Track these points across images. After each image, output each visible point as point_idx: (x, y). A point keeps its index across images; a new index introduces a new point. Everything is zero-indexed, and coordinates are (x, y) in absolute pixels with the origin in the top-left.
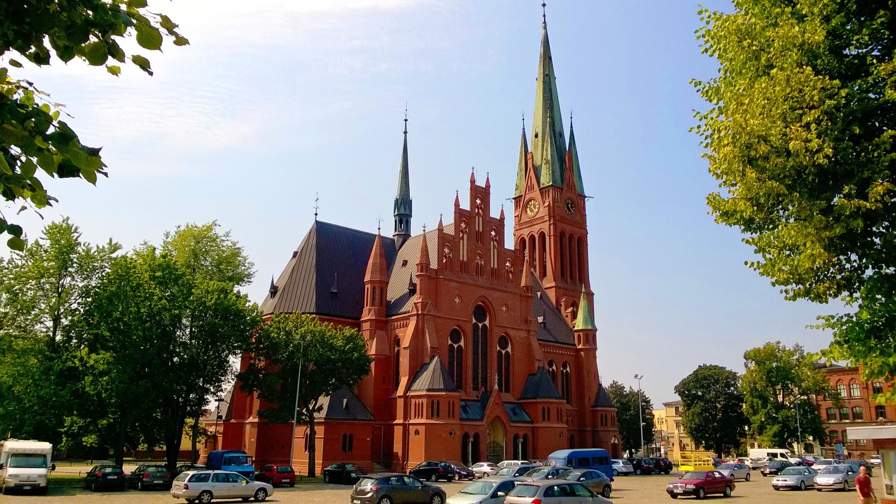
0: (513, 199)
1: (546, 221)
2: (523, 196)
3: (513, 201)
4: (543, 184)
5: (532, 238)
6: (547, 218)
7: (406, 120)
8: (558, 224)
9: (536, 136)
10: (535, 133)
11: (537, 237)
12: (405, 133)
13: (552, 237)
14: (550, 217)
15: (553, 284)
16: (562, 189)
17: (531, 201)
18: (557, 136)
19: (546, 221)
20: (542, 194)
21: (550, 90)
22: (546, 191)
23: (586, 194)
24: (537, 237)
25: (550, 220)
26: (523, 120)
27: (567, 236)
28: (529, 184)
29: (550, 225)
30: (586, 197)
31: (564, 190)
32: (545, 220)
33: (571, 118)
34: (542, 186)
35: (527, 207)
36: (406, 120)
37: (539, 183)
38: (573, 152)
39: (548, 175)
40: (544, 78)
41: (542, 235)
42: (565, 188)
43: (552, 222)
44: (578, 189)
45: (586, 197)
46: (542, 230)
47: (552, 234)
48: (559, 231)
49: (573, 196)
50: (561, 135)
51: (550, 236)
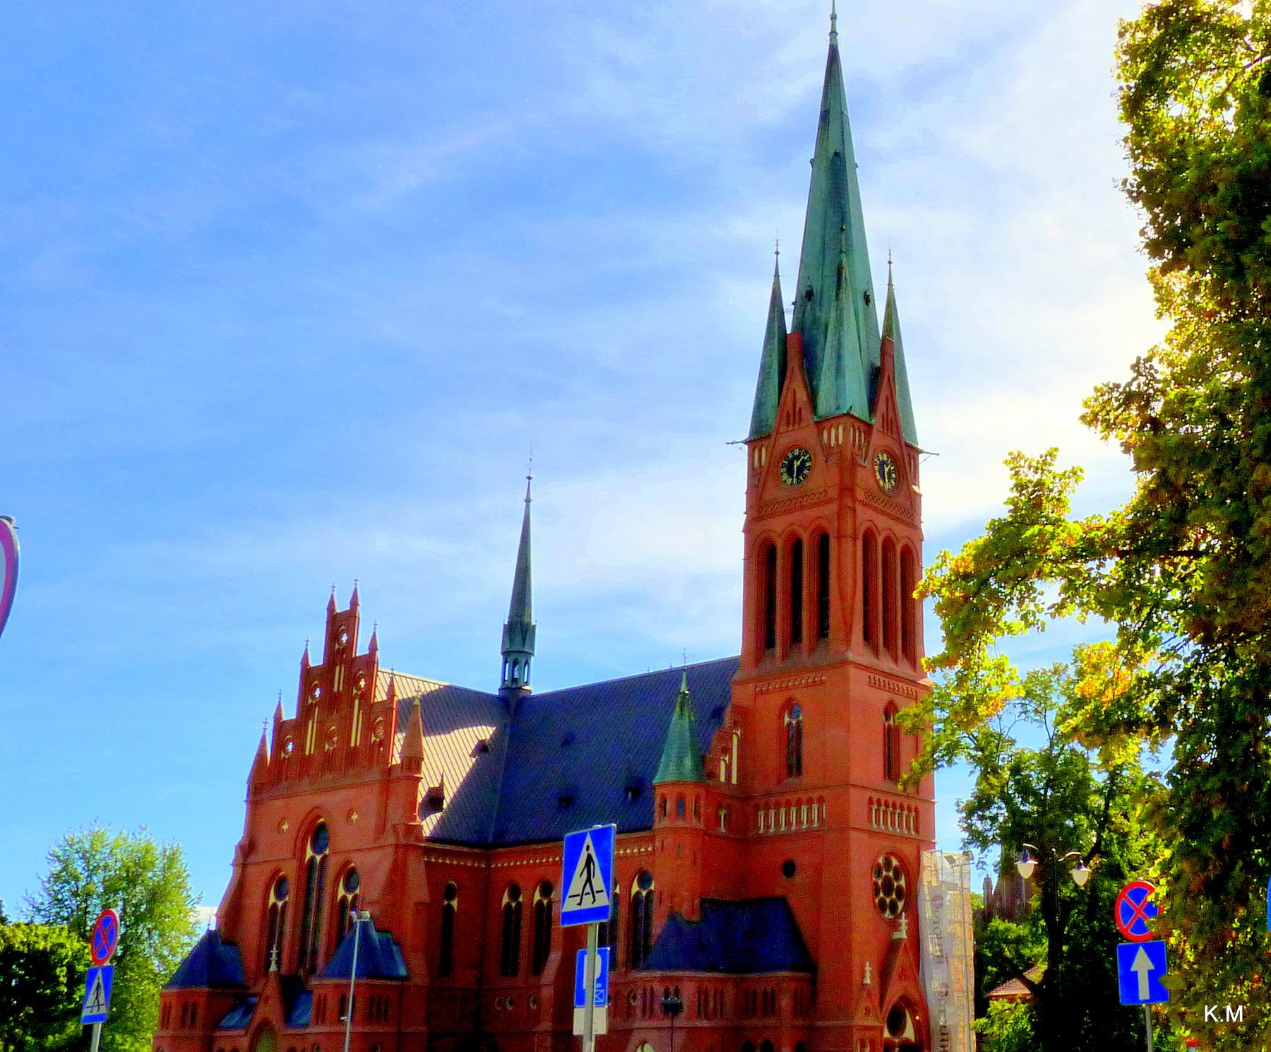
0: (746, 442)
23: (920, 447)
30: (919, 452)
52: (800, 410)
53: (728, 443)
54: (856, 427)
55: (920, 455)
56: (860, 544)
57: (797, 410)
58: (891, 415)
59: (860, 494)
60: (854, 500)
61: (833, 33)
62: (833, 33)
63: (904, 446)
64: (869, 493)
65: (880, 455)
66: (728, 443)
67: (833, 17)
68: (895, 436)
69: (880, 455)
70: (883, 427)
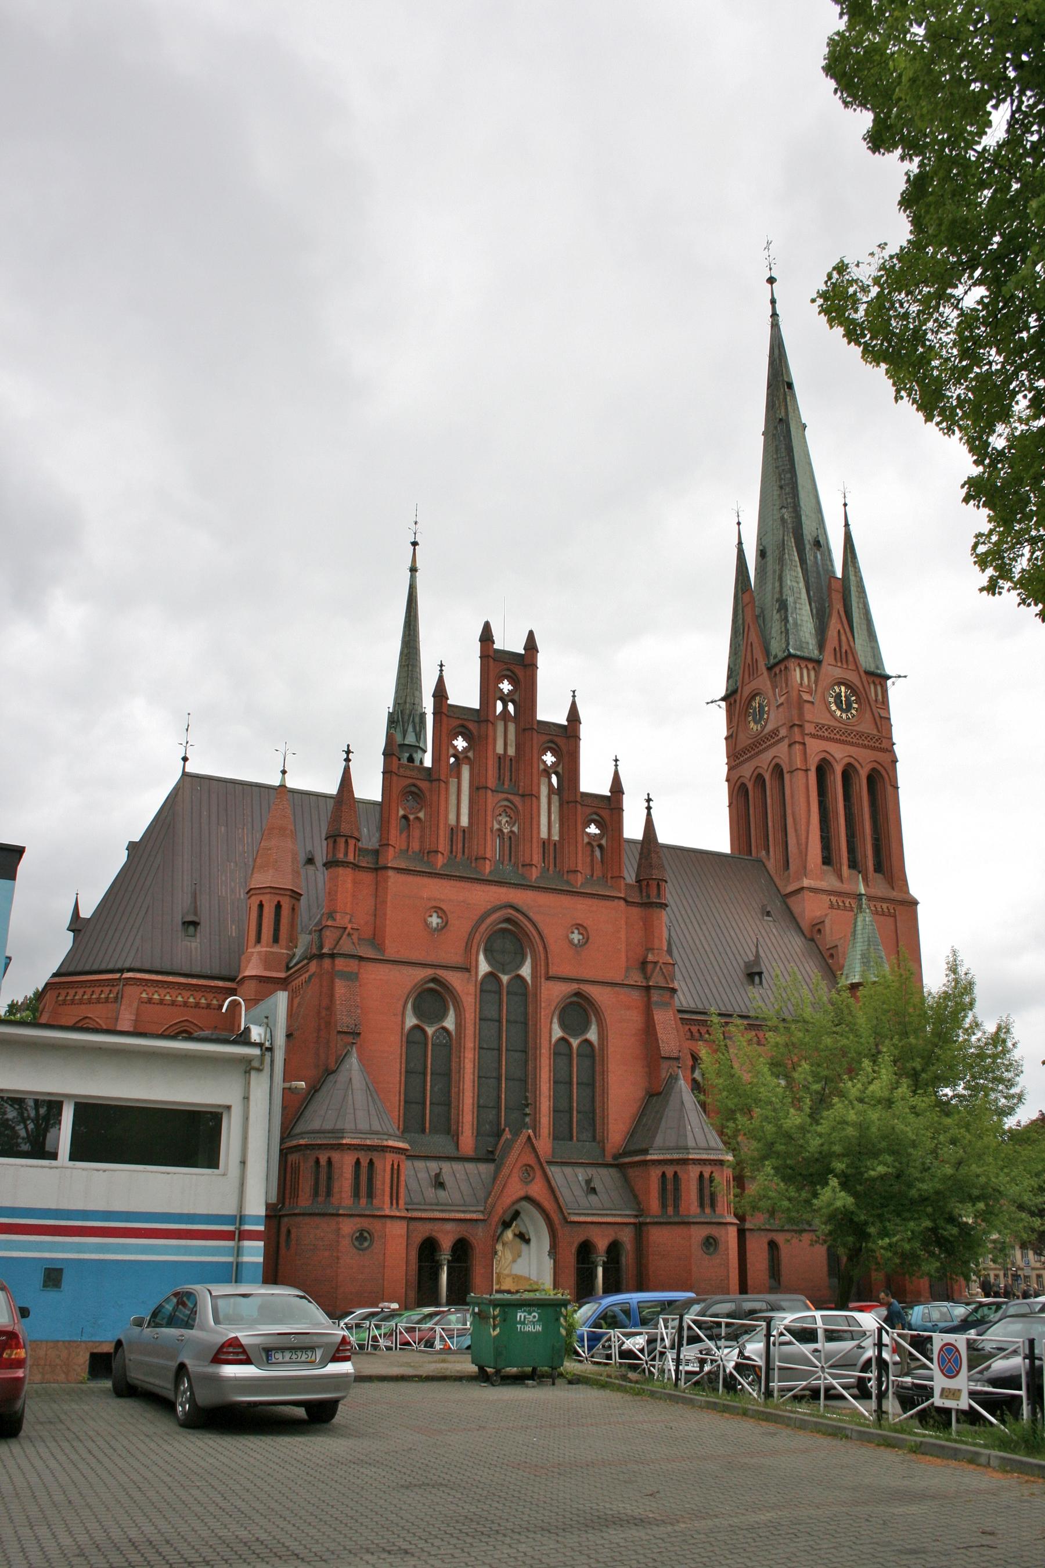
0: (722, 699)
3: (723, 704)
4: (776, 656)
5: (760, 779)
7: (415, 544)
8: (808, 740)
12: (413, 570)
16: (819, 662)
17: (753, 698)
18: (808, 547)
21: (790, 450)
22: (781, 671)
23: (889, 670)
27: (838, 769)
28: (749, 660)
29: (790, 745)
30: (889, 677)
31: (824, 664)
32: (781, 736)
33: (845, 505)
36: (415, 544)
37: (767, 652)
38: (852, 578)
39: (784, 635)
40: (776, 428)
42: (828, 657)
44: (865, 661)
45: (889, 677)
46: (776, 760)
49: (852, 677)
50: (820, 544)
53: (708, 703)
55: (889, 682)
56: (812, 775)
58: (845, 647)
59: (809, 728)
60: (803, 734)
61: (774, 315)
62: (774, 315)
63: (862, 674)
64: (820, 726)
65: (836, 687)
66: (708, 703)
67: (773, 302)
69: (836, 687)
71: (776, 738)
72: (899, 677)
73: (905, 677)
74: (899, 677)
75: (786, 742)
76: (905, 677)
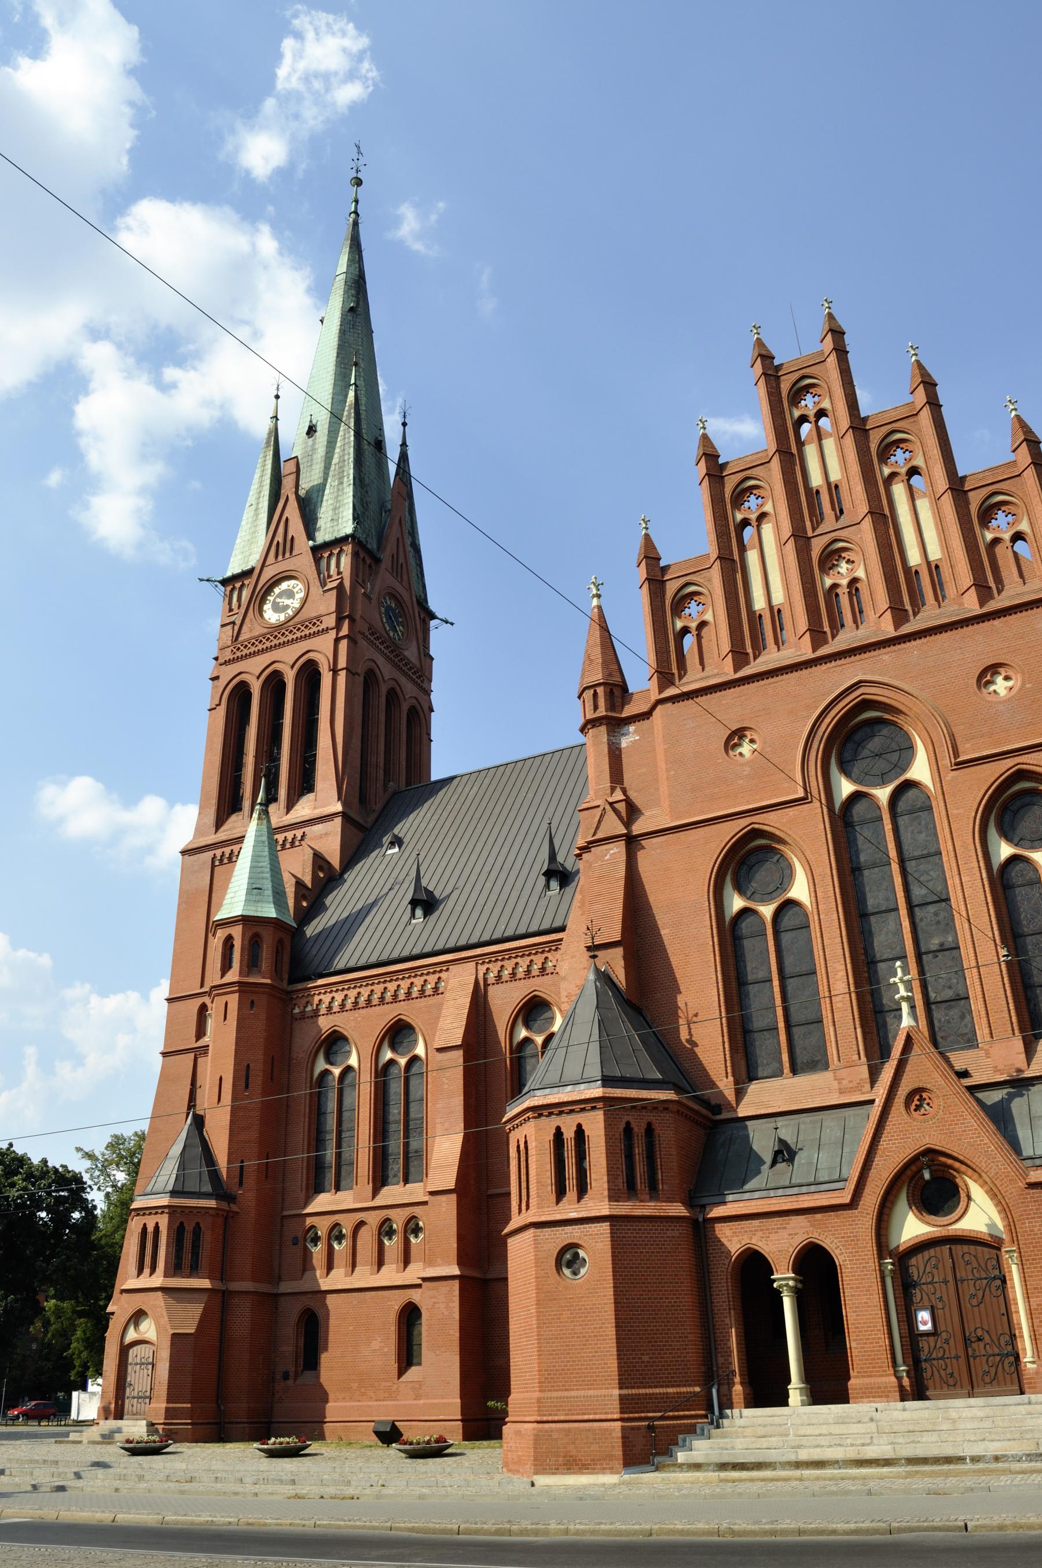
1: (327, 630)
2: (257, 572)
6: (330, 621)
9: (311, 430)
10: (307, 424)
11: (290, 677)
13: (343, 674)
14: (339, 621)
15: (338, 807)
19: (327, 630)
20: (317, 561)
24: (290, 677)
25: (338, 627)
26: (277, 397)
28: (279, 538)
29: (337, 640)
30: (433, 617)
32: (323, 626)
34: (321, 537)
35: (263, 601)
41: (310, 674)
43: (345, 631)
46: (311, 655)
47: (342, 663)
48: (361, 670)
51: (335, 671)
52: (293, 537)
53: (201, 580)
54: (362, 556)
55: (433, 623)
57: (289, 537)
58: (401, 560)
66: (201, 580)
68: (405, 583)
70: (392, 568)
71: (315, 629)
72: (447, 622)
73: (452, 624)
74: (447, 622)
75: (333, 634)
76: (452, 624)
